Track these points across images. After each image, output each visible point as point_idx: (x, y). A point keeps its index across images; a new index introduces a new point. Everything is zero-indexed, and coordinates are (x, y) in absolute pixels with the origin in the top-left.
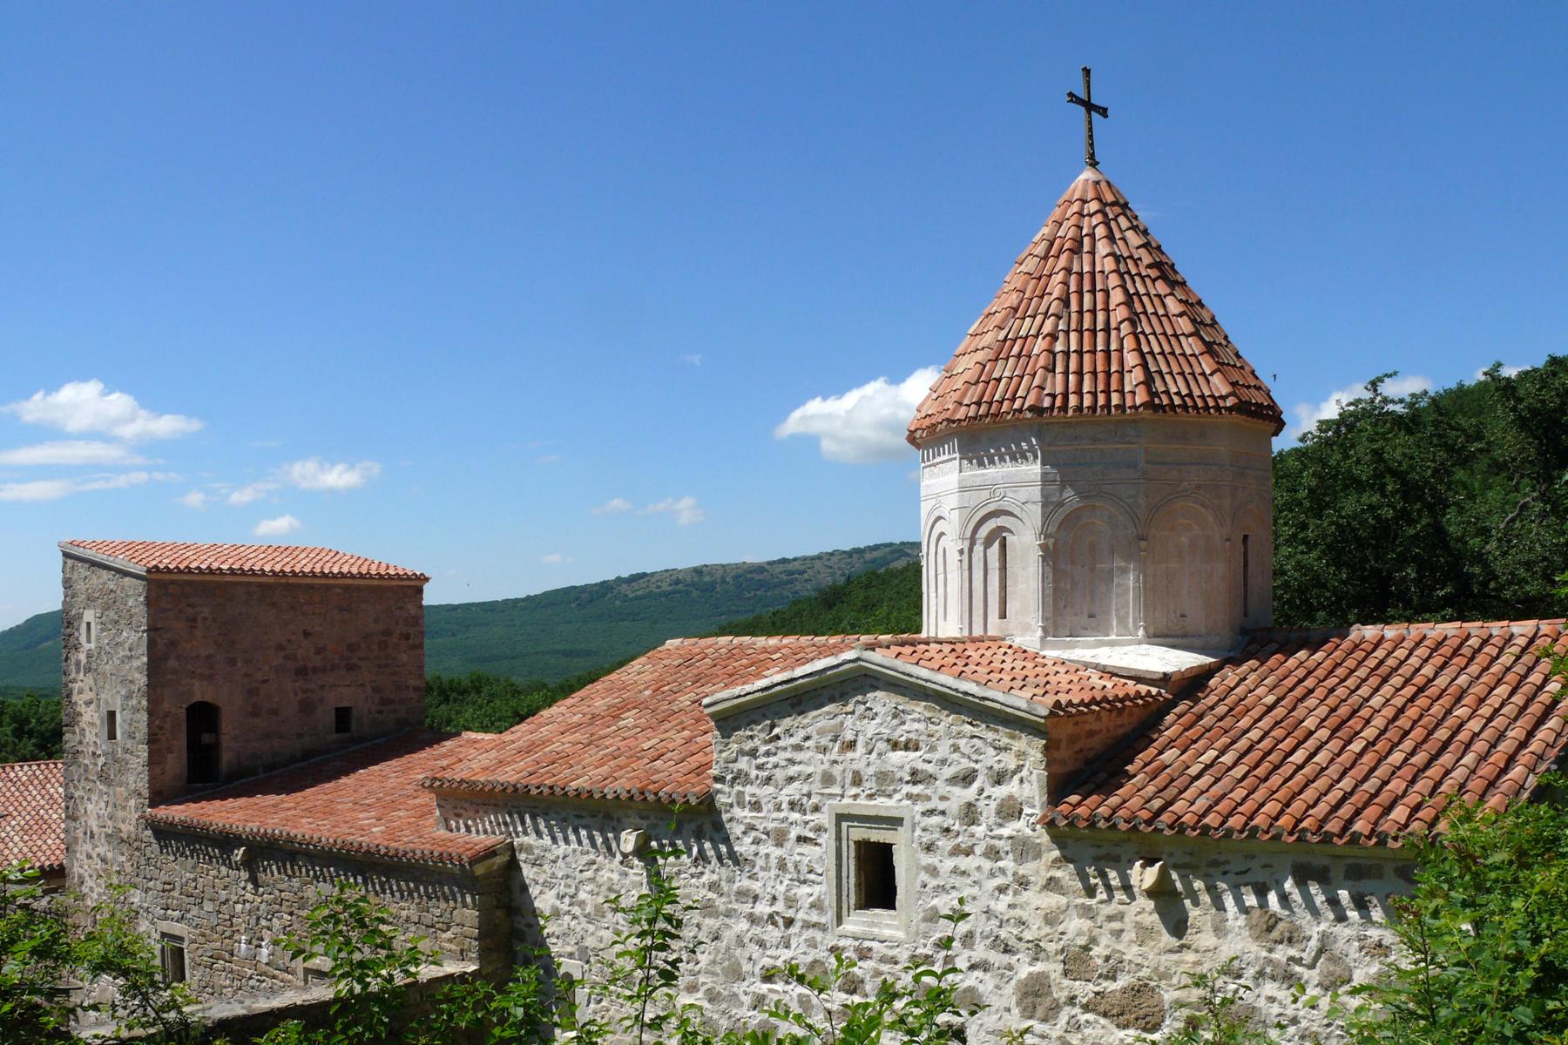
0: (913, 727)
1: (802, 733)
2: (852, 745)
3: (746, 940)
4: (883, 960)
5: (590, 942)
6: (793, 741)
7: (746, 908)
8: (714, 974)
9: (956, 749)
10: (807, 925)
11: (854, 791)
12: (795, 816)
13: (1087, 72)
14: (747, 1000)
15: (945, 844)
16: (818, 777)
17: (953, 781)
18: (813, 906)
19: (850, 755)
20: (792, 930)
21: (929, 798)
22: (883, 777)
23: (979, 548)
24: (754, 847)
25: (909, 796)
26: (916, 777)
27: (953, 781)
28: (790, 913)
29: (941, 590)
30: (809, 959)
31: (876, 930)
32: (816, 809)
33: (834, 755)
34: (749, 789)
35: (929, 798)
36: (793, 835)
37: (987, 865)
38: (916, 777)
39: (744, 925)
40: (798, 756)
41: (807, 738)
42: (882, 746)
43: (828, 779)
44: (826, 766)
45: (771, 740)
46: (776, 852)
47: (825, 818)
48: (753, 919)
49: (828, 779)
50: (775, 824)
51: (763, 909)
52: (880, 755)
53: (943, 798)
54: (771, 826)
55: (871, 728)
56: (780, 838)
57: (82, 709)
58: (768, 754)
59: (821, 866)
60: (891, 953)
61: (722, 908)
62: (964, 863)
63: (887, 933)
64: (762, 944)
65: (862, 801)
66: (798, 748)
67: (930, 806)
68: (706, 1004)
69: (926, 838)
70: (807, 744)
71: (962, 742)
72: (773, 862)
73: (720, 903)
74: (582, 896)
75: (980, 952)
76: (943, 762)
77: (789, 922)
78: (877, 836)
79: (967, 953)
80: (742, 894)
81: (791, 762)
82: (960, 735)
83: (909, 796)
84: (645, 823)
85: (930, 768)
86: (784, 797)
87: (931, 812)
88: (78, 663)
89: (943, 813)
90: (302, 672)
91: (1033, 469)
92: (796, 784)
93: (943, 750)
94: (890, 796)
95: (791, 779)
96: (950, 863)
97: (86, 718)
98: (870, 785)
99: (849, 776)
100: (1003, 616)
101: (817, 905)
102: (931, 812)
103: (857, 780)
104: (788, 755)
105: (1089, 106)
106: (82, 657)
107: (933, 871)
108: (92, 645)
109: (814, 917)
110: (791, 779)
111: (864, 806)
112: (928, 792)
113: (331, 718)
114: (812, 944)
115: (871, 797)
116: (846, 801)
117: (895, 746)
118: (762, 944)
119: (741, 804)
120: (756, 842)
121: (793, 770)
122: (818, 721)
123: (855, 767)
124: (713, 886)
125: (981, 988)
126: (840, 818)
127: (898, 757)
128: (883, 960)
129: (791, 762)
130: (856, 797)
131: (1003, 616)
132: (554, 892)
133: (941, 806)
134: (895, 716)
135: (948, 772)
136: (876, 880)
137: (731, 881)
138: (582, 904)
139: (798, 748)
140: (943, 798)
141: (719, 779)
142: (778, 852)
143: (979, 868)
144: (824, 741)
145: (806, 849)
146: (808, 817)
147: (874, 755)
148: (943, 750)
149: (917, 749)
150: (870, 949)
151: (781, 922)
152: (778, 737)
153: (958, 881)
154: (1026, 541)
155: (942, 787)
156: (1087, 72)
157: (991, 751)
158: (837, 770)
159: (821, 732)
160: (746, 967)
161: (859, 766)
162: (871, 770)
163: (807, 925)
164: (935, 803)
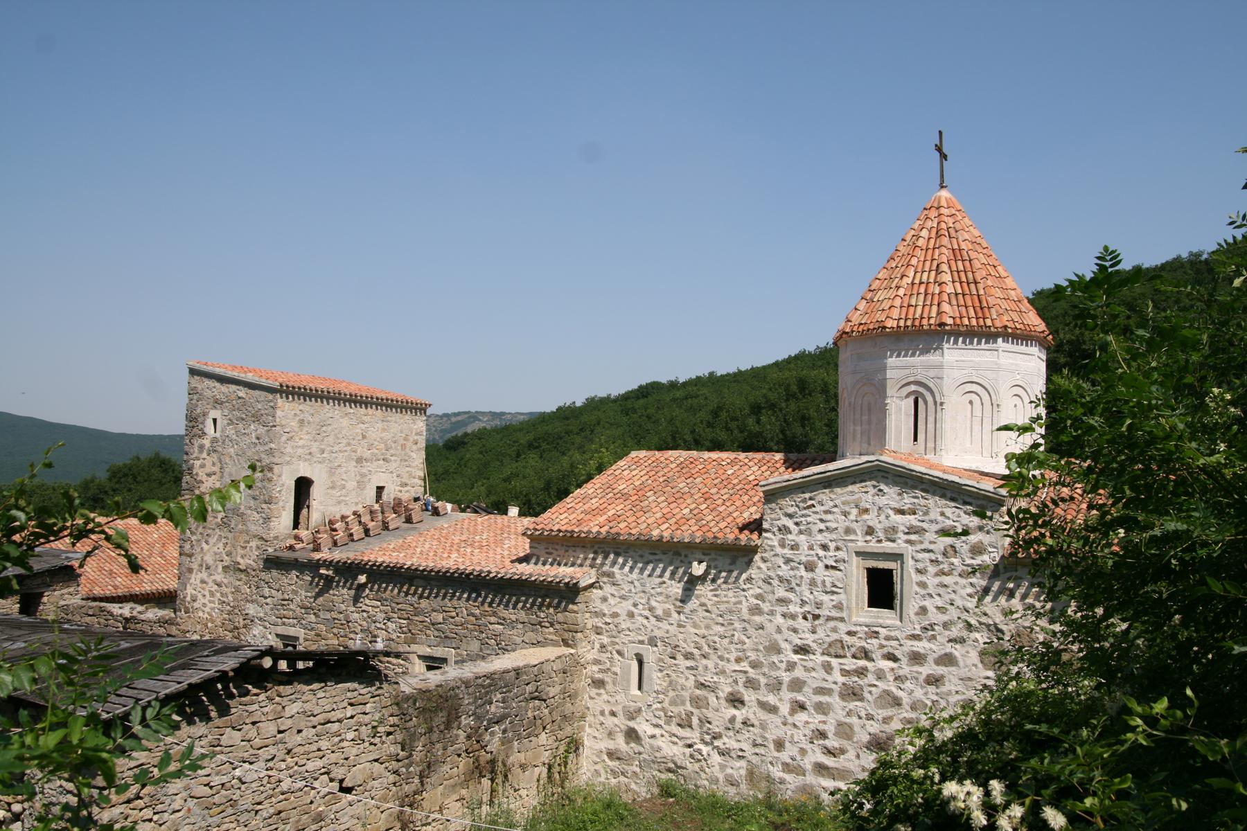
1: (831, 504)
2: (866, 511)
4: (888, 638)
5: (657, 633)
6: (823, 508)
7: (784, 609)
8: (757, 650)
9: (942, 514)
10: (829, 619)
11: (869, 538)
12: (821, 553)
13: (940, 133)
14: (783, 666)
15: (932, 569)
18: (834, 607)
19: (865, 517)
20: (817, 622)
21: (922, 542)
24: (792, 573)
25: (909, 542)
28: (817, 612)
30: (832, 639)
31: (881, 621)
32: (838, 549)
33: (852, 517)
34: (790, 537)
36: (821, 565)
37: (963, 581)
38: (912, 530)
40: (829, 517)
42: (891, 513)
43: (848, 531)
45: (809, 507)
46: (807, 576)
50: (810, 558)
51: (793, 608)
52: (887, 517)
53: (931, 542)
54: (804, 559)
55: (882, 501)
56: (810, 567)
58: (803, 516)
60: (893, 634)
61: (766, 610)
62: (947, 580)
63: (889, 622)
64: (795, 631)
66: (826, 512)
67: (923, 547)
68: (750, 670)
70: (835, 510)
72: (806, 581)
73: (766, 607)
74: (654, 604)
75: (955, 632)
77: (816, 617)
79: (947, 633)
80: (782, 601)
81: (822, 520)
84: (707, 558)
85: (925, 525)
87: (925, 550)
88: (201, 447)
89: (931, 551)
90: (359, 460)
91: (892, 361)
93: (934, 514)
94: (893, 541)
96: (937, 580)
98: (881, 535)
101: (839, 607)
102: (925, 550)
103: (870, 531)
106: (207, 442)
107: (923, 585)
108: (218, 435)
109: (834, 614)
110: (821, 531)
111: (873, 546)
113: (373, 493)
114: (835, 630)
115: (880, 541)
116: (860, 544)
118: (795, 631)
119: (783, 546)
121: (822, 526)
123: (870, 524)
124: (758, 597)
125: (956, 653)
128: (888, 638)
132: (631, 602)
133: (931, 547)
134: (900, 494)
135: (935, 527)
136: (882, 590)
138: (651, 609)
139: (826, 512)
140: (931, 542)
142: (810, 575)
143: (956, 583)
144: (847, 509)
145: (833, 572)
146: (831, 554)
149: (915, 513)
150: (877, 633)
151: (810, 617)
153: (941, 591)
155: (930, 536)
156: (940, 133)
158: (854, 525)
160: (784, 645)
163: (829, 619)
164: (926, 545)
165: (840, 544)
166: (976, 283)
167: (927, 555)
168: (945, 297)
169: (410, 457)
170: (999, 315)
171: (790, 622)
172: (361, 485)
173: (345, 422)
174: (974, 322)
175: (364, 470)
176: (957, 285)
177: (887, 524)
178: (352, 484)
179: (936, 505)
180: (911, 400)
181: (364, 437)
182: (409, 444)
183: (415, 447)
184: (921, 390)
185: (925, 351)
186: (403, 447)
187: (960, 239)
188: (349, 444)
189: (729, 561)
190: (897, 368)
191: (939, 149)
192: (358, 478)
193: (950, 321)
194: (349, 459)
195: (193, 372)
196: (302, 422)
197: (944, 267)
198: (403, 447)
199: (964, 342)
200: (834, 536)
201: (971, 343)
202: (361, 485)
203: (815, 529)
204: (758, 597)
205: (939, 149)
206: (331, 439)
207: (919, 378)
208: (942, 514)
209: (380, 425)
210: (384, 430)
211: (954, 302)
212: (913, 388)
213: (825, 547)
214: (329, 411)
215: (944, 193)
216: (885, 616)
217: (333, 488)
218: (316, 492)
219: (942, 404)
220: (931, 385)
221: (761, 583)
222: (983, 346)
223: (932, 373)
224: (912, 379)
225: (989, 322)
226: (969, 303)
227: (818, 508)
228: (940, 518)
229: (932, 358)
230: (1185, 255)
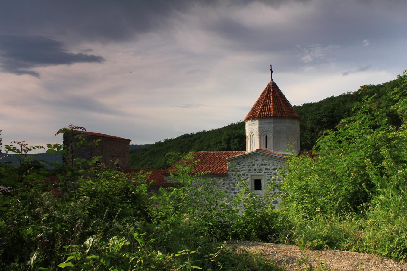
0: (265, 161)
1: (245, 163)
3: (233, 196)
6: (243, 164)
7: (234, 191)
9: (273, 165)
11: (254, 172)
12: (244, 176)
13: (271, 65)
16: (248, 170)
17: (273, 170)
19: (254, 166)
21: (268, 172)
22: (260, 170)
23: (262, 137)
25: (265, 172)
26: (266, 169)
27: (273, 170)
29: (253, 143)
32: (247, 175)
35: (268, 172)
38: (266, 169)
39: (233, 194)
40: (244, 167)
41: (246, 164)
43: (250, 170)
44: (249, 168)
47: (249, 176)
48: (235, 193)
49: (250, 170)
52: (259, 166)
55: (258, 162)
58: (238, 167)
59: (249, 182)
60: (261, 196)
63: (261, 193)
65: (256, 173)
66: (244, 166)
67: (268, 173)
69: (268, 178)
71: (274, 164)
73: (228, 191)
76: (271, 167)
78: (258, 178)
80: (233, 189)
82: (274, 163)
83: (265, 172)
85: (268, 168)
86: (241, 173)
89: (271, 174)
92: (243, 171)
93: (271, 165)
95: (242, 171)
98: (257, 171)
99: (254, 170)
100: (266, 147)
104: (242, 167)
112: (268, 171)
117: (262, 165)
120: (235, 181)
122: (248, 161)
123: (255, 168)
126: (252, 176)
127: (263, 166)
129: (243, 168)
130: (255, 173)
131: (266, 147)
133: (270, 173)
135: (272, 168)
137: (230, 187)
139: (244, 166)
141: (228, 171)
144: (249, 164)
147: (258, 166)
148: (271, 165)
152: (240, 164)
154: (270, 136)
155: (270, 170)
156: (271, 65)
157: (279, 165)
158: (251, 169)
159: (248, 163)
161: (256, 168)
162: (258, 168)
164: (269, 173)
165: (247, 173)
167: (269, 176)
171: (235, 195)
177: (259, 168)
179: (272, 163)
180: (265, 137)
189: (218, 179)
191: (271, 70)
200: (245, 172)
203: (240, 170)
204: (227, 188)
205: (271, 70)
208: (273, 165)
213: (243, 175)
216: (260, 192)
221: (227, 185)
227: (242, 165)
228: (273, 166)
230: (297, 106)
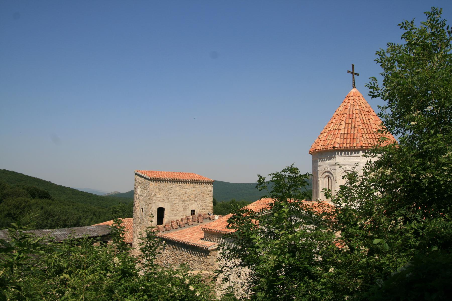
13: (353, 65)
57: (137, 207)
90: (184, 201)
97: (137, 210)
105: (353, 73)
113: (190, 212)
156: (353, 65)
166: (355, 128)
168: (339, 135)
169: (206, 199)
170: (360, 141)
172: (185, 209)
173: (177, 189)
174: (348, 145)
175: (186, 205)
176: (346, 129)
178: (181, 209)
181: (186, 193)
182: (205, 195)
183: (208, 196)
184: (329, 174)
185: (330, 159)
186: (203, 196)
187: (354, 109)
188: (179, 196)
190: (321, 166)
192: (183, 207)
193: (337, 145)
194: (180, 201)
195: (136, 174)
196: (160, 189)
197: (343, 123)
198: (203, 196)
199: (345, 154)
201: (348, 154)
202: (185, 209)
206: (172, 195)
207: (328, 170)
209: (192, 189)
210: (194, 191)
211: (342, 137)
212: (327, 174)
214: (170, 185)
215: (354, 90)
217: (173, 211)
218: (166, 212)
219: (336, 180)
220: (332, 172)
222: (353, 155)
223: (332, 168)
224: (326, 170)
225: (355, 145)
226: (349, 137)
229: (333, 161)
